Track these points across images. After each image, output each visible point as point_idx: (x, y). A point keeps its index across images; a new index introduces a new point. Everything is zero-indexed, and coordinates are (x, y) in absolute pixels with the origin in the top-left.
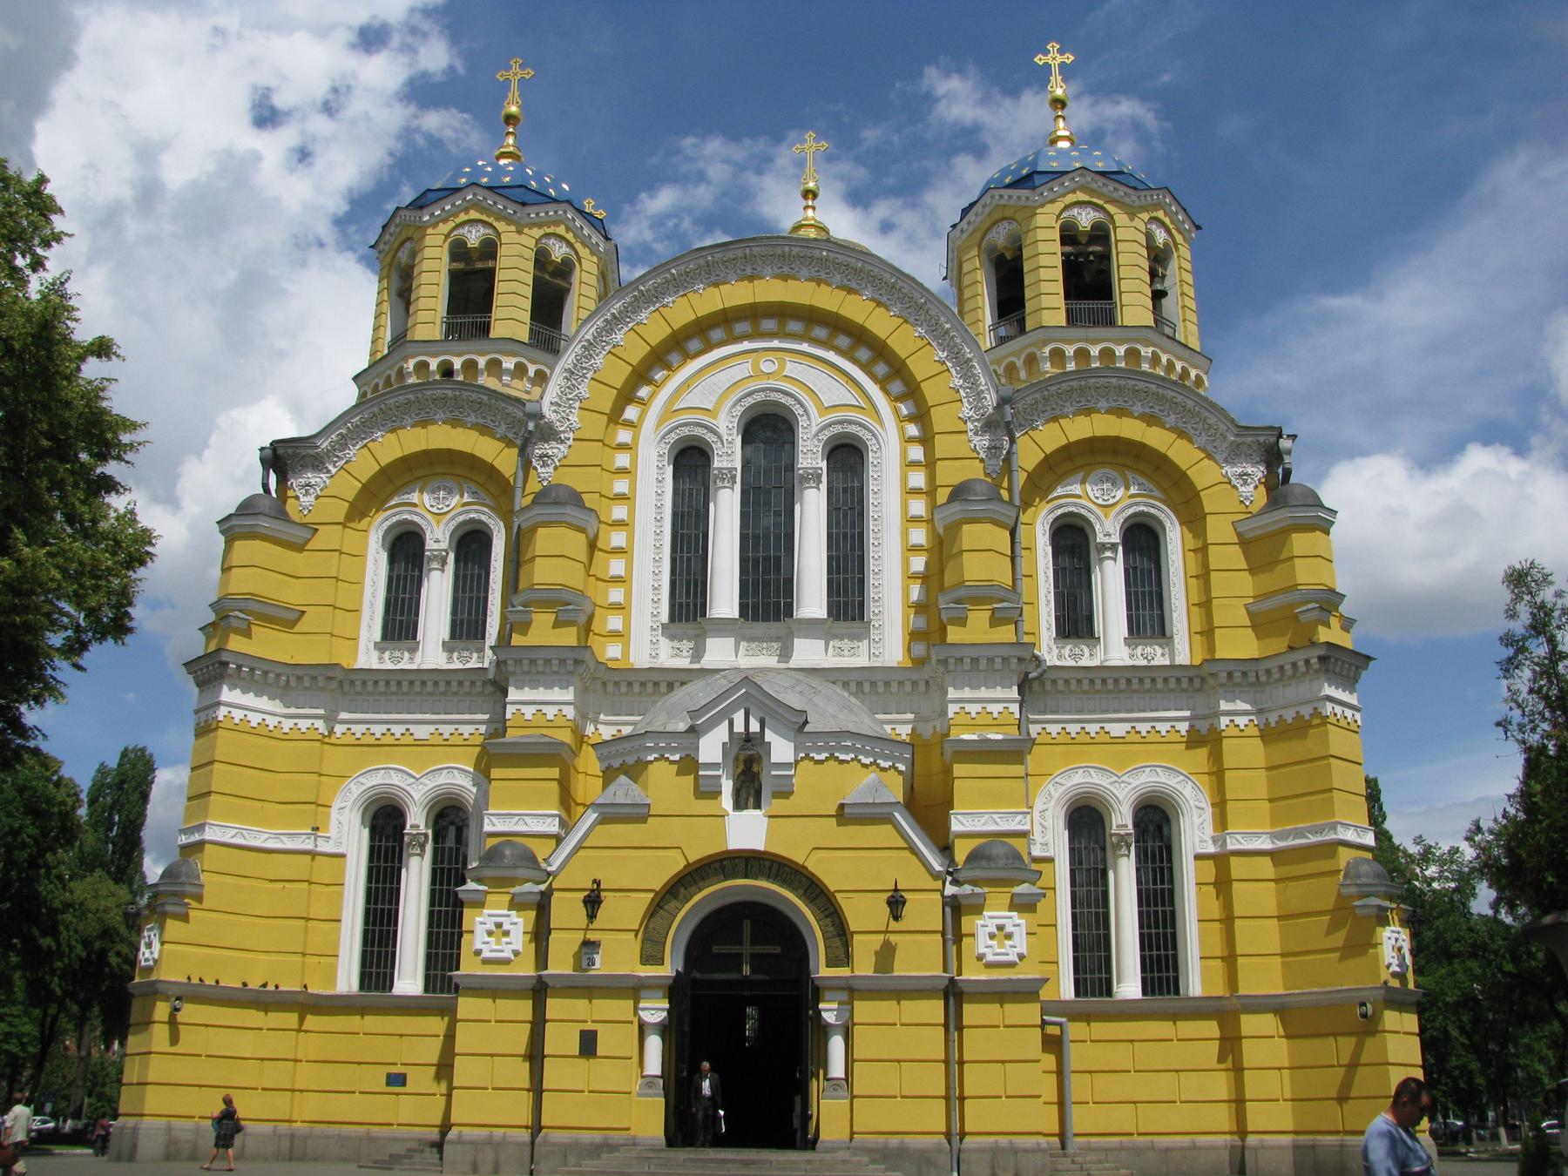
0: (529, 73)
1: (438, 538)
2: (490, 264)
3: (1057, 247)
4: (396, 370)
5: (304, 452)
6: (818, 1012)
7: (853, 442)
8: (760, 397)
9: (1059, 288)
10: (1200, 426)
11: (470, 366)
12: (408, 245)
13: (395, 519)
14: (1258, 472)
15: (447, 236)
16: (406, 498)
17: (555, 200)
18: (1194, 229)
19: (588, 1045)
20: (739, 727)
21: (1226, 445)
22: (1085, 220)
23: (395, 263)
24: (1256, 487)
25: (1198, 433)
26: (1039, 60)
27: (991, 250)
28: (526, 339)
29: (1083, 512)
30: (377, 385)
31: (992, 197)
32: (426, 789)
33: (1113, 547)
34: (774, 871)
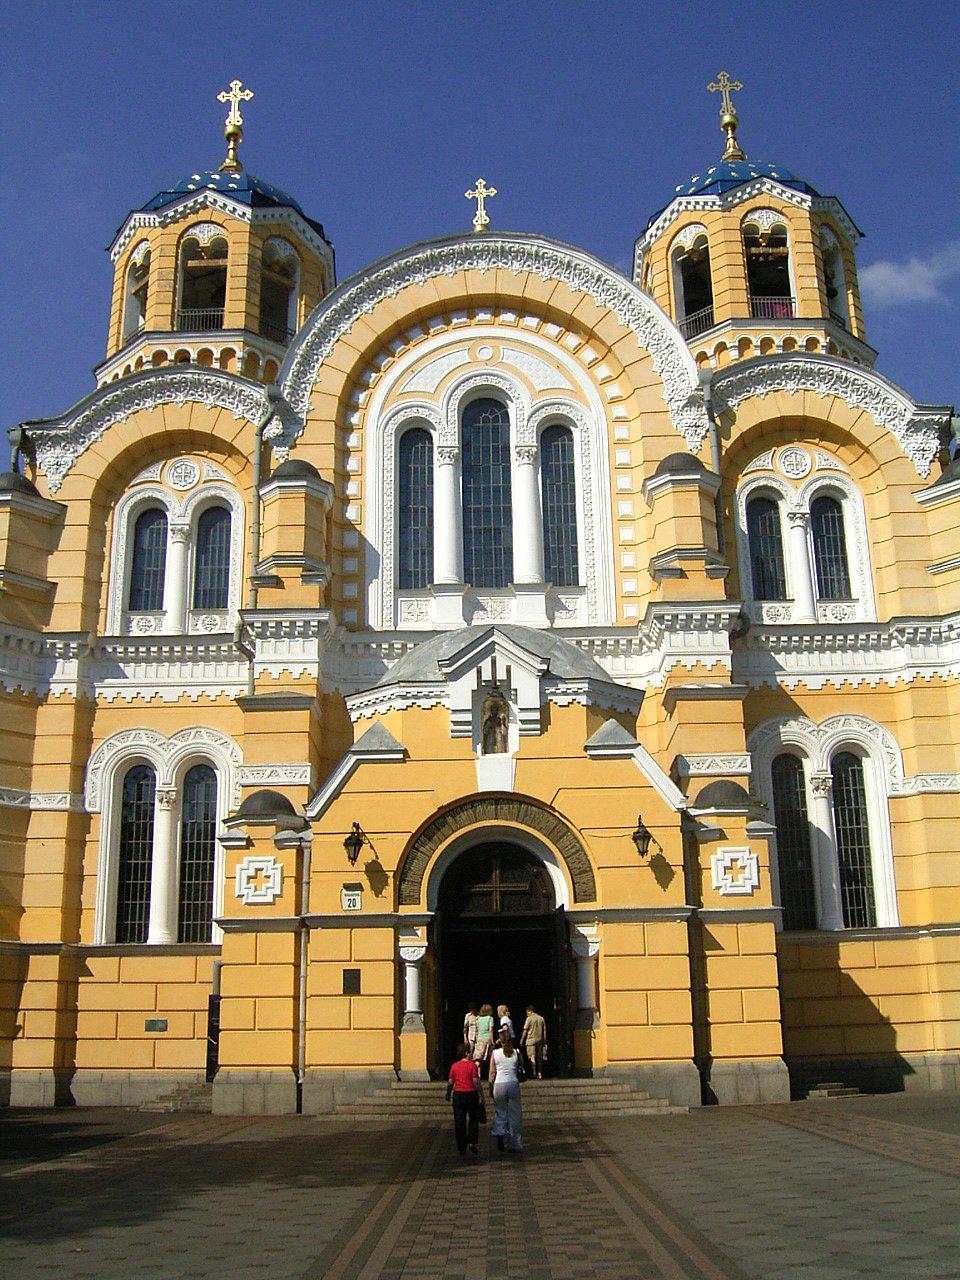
0: (248, 95)
1: (180, 515)
2: (221, 262)
3: (739, 247)
4: (135, 360)
5: (53, 433)
6: (570, 945)
7: (562, 423)
8: (479, 382)
9: (743, 284)
10: (879, 406)
11: (205, 355)
12: (143, 246)
13: (139, 497)
14: (934, 444)
15: (181, 236)
16: (144, 476)
17: (279, 205)
18: (858, 235)
19: (352, 983)
20: (487, 675)
22: (764, 223)
23: (130, 264)
24: (931, 462)
25: (878, 412)
26: (711, 87)
27: (680, 250)
28: (258, 332)
29: (775, 485)
30: (117, 375)
31: (680, 204)
32: (176, 749)
33: (804, 514)
34: (522, 812)
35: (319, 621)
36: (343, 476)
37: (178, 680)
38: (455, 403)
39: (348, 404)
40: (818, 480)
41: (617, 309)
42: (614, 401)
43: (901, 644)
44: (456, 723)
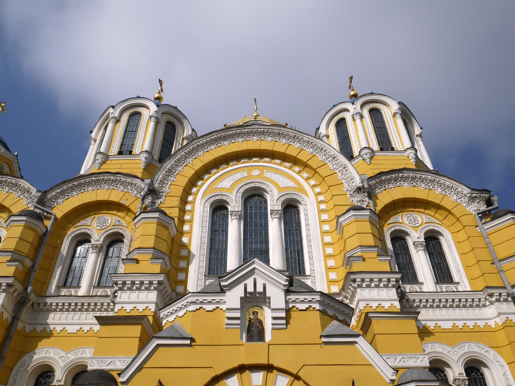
20: (250, 289)
21: (467, 198)
35: (159, 281)
36: (182, 222)
37: (77, 321)
38: (240, 195)
39: (187, 191)
40: (425, 227)
41: (318, 155)
42: (319, 194)
43: (492, 303)
44: (229, 318)
